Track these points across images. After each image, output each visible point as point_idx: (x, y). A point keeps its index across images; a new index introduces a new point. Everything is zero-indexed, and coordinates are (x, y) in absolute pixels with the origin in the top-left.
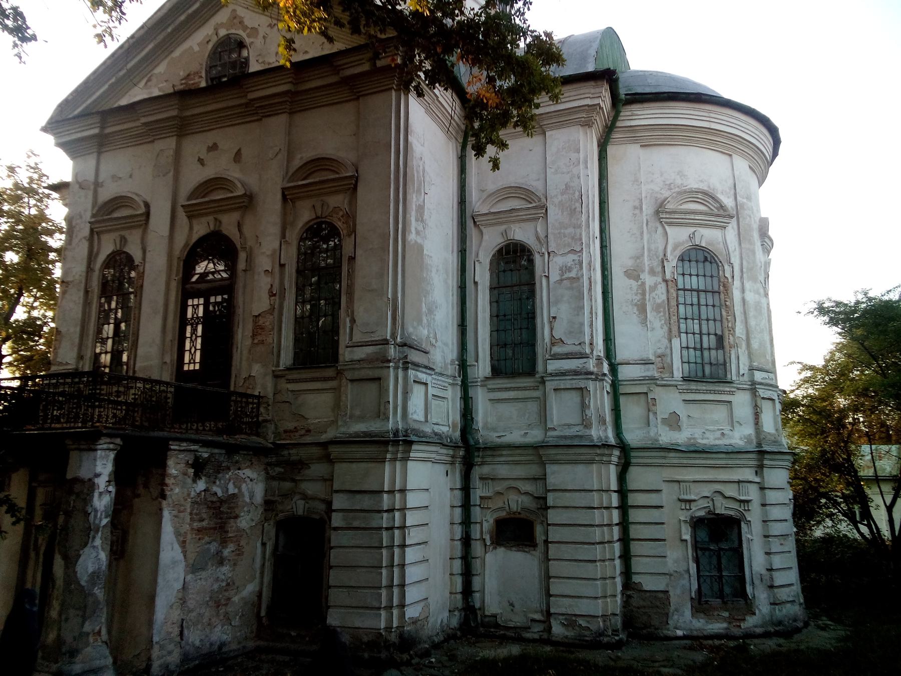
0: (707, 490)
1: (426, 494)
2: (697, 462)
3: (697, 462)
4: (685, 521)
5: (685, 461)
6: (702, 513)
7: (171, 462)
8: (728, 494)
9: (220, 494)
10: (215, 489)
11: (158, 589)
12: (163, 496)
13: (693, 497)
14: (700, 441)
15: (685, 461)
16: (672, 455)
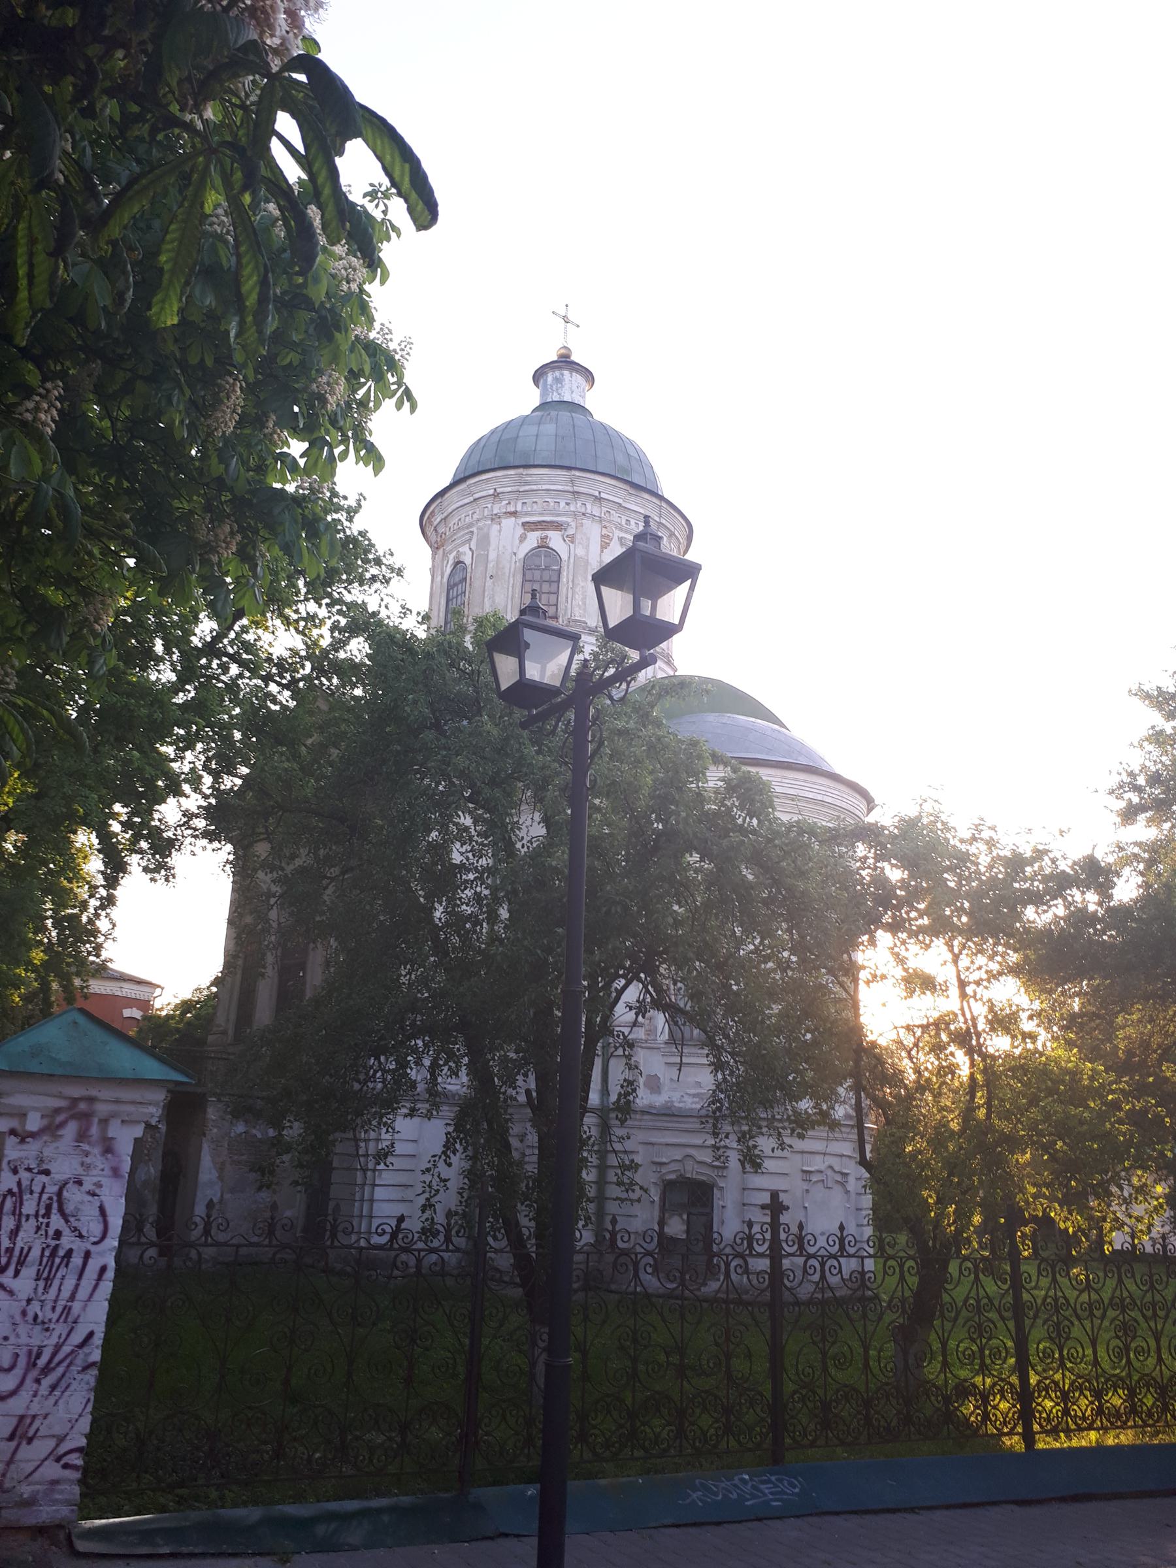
0: (678, 1154)
1: (414, 1145)
2: (670, 1125)
3: (670, 1125)
4: (655, 1183)
5: (659, 1124)
6: (672, 1177)
7: (210, 1110)
8: (699, 1158)
9: (259, 1136)
10: (254, 1131)
11: (197, 1200)
12: (204, 1135)
13: (664, 1160)
14: (676, 1104)
15: (659, 1124)
16: (646, 1117)
